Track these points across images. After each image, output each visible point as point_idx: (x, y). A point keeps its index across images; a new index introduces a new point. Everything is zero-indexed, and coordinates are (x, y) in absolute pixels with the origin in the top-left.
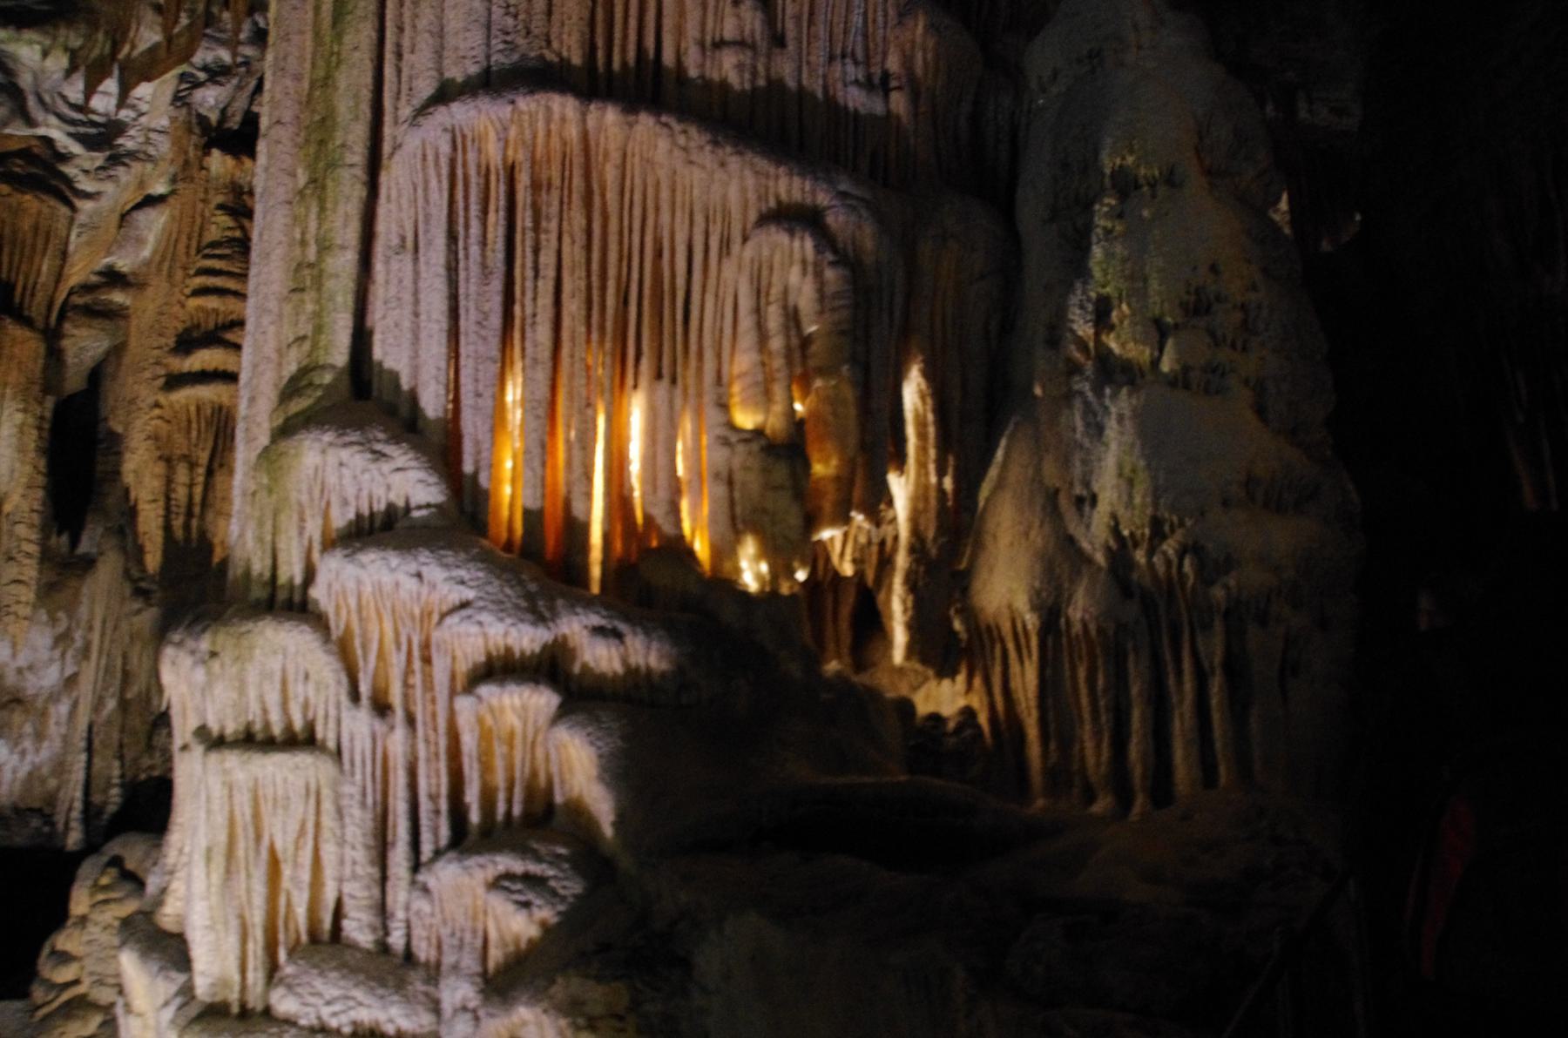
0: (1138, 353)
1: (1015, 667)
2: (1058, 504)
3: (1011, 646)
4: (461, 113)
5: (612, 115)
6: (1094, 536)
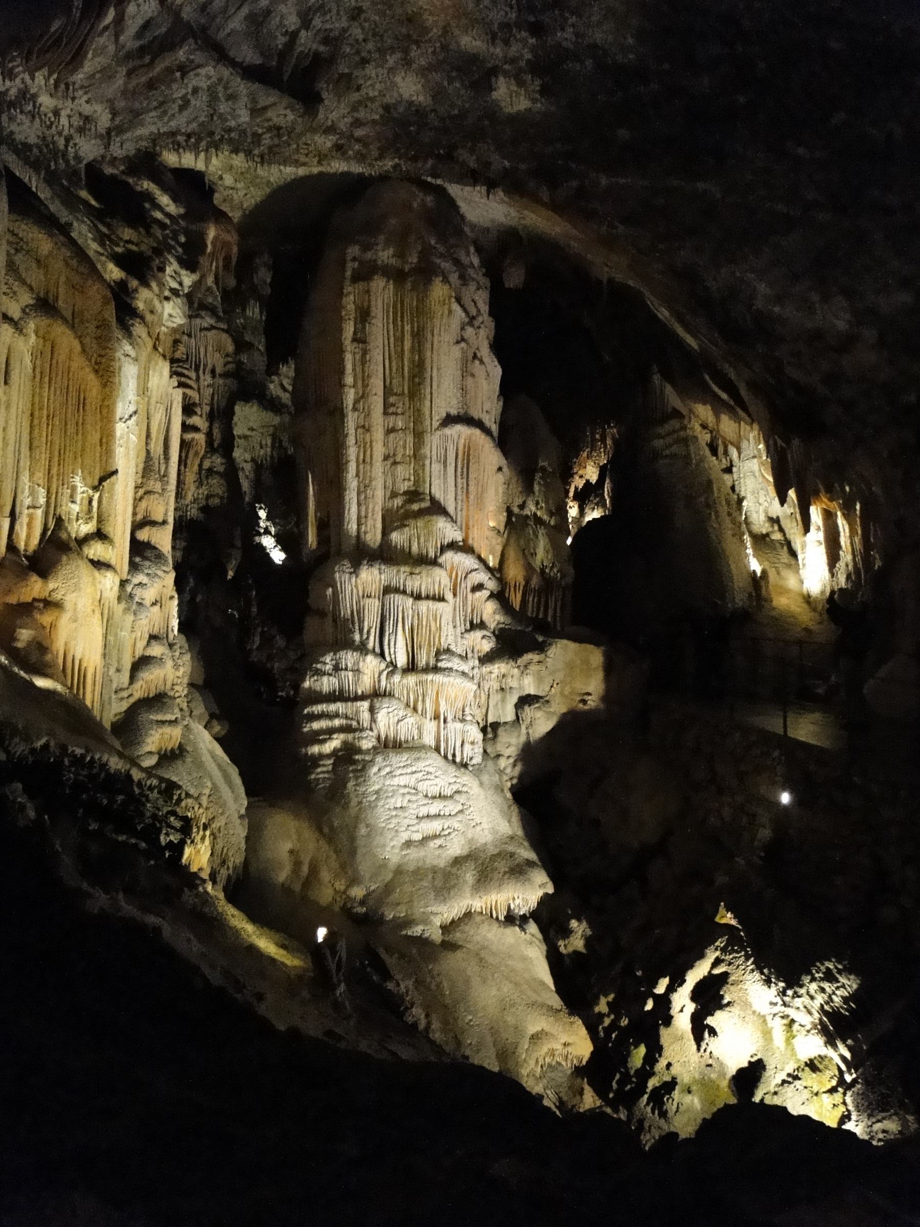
2: (527, 554)
3: (512, 589)
4: (459, 428)
6: (537, 563)
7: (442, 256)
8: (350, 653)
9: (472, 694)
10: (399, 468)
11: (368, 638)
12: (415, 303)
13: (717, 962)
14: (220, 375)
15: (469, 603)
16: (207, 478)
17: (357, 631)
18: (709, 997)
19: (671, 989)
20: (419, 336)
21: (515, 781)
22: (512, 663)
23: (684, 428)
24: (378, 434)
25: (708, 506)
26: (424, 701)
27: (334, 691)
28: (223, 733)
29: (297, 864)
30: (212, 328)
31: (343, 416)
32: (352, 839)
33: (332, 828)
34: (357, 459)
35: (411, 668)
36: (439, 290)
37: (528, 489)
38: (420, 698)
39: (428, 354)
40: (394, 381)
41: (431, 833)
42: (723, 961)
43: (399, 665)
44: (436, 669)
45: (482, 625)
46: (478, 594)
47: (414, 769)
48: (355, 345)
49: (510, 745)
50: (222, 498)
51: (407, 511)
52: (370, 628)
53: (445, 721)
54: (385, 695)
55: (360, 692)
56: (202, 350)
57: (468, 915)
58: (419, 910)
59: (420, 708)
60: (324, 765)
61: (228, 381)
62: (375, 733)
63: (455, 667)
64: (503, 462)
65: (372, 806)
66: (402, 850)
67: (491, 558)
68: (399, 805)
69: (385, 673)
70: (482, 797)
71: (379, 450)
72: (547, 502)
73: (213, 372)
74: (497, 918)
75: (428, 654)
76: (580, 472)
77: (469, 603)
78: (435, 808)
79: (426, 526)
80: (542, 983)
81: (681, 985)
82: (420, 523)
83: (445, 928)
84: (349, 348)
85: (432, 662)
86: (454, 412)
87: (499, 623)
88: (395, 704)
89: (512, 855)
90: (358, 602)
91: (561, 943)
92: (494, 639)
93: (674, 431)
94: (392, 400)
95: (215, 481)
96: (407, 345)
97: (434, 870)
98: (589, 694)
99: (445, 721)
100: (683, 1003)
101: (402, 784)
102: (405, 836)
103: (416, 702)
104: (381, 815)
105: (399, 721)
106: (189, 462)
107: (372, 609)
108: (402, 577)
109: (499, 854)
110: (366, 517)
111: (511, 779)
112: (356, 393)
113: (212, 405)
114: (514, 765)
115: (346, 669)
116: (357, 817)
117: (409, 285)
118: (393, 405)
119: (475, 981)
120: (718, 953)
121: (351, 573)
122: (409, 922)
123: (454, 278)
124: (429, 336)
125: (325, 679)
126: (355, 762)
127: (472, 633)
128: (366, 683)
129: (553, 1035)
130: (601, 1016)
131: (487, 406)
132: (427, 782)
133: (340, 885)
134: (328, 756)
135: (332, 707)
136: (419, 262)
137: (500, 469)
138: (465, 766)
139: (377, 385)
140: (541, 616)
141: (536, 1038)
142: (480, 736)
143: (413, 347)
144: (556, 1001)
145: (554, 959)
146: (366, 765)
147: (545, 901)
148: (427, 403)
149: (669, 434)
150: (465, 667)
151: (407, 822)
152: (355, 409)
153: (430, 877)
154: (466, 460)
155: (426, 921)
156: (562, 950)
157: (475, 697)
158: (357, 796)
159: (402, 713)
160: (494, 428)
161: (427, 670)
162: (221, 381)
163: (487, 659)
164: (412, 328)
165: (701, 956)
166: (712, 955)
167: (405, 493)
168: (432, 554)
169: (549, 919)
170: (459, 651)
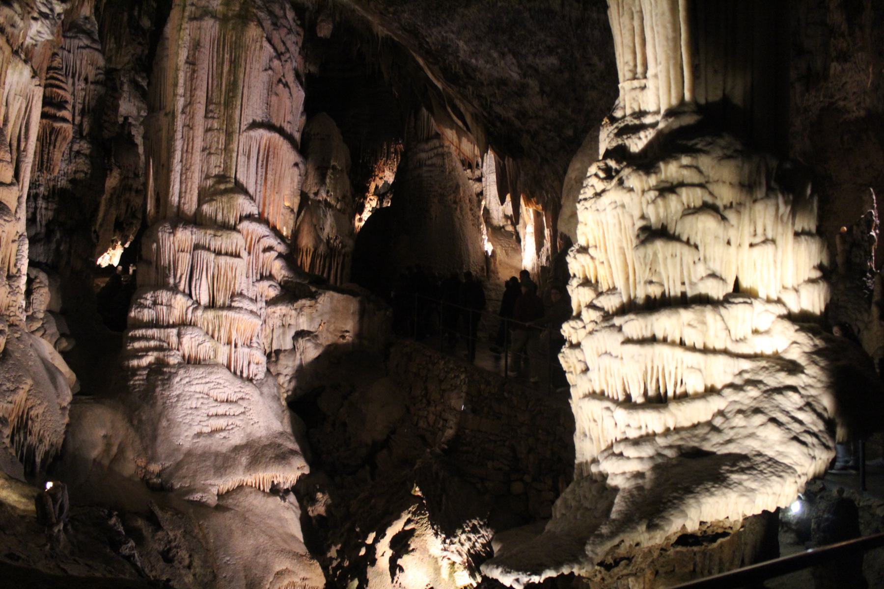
0: (333, 202)
1: (305, 257)
2: (317, 229)
5: (282, 139)
6: (324, 236)
7: (259, 8)
8: (164, 293)
9: (259, 327)
10: (213, 158)
11: (180, 282)
12: (234, 39)
13: (409, 521)
14: (92, 83)
15: (261, 260)
16: (75, 157)
17: (172, 276)
18: (401, 545)
19: (376, 540)
20: (235, 64)
21: (290, 393)
22: (290, 306)
23: (442, 146)
24: (199, 131)
25: (455, 202)
26: (219, 330)
27: (153, 320)
28: (70, 347)
29: (109, 446)
30: (87, 47)
31: (174, 117)
32: (155, 429)
33: (140, 421)
34: (182, 150)
35: (212, 305)
36: (253, 31)
37: (322, 181)
38: (217, 329)
39: (242, 76)
40: (214, 94)
41: (219, 427)
42: (413, 521)
43: (202, 303)
44: (230, 308)
45: (271, 277)
46: (267, 254)
47: (207, 380)
48: (187, 66)
49: (287, 367)
50: (86, 174)
51: (215, 190)
52: (182, 275)
53: (236, 346)
54: (190, 325)
55: (171, 322)
56: (78, 63)
57: (240, 487)
58: (201, 481)
59: (216, 336)
60: (140, 375)
61: (99, 87)
62: (181, 353)
63: (245, 307)
64: (298, 159)
65: (173, 406)
66: (193, 438)
67: (285, 229)
68: (194, 406)
69: (191, 308)
70: (261, 403)
71: (199, 143)
72: (335, 192)
73: (86, 80)
74: (264, 490)
75: (225, 296)
76: (380, 175)
77: (261, 260)
78: (222, 409)
79: (229, 201)
80: (294, 537)
81: (383, 537)
82: (225, 199)
83: (220, 496)
84: (182, 68)
85: (228, 302)
86: (259, 119)
87: (284, 277)
88: (196, 332)
89: (280, 445)
90: (174, 256)
91: (310, 509)
92: (279, 288)
93: (436, 148)
94: (211, 107)
95: (80, 161)
96: (226, 68)
97: (217, 454)
98: (347, 331)
99: (236, 346)
100: (384, 549)
101: (198, 390)
102: (196, 429)
103: (213, 331)
104: (180, 413)
105: (199, 344)
106: (58, 144)
107: (184, 260)
108: (208, 238)
109: (270, 445)
110: (185, 192)
111: (287, 391)
112: (186, 101)
113: (84, 103)
114: (290, 381)
115: (162, 304)
116: (160, 414)
117: (230, 26)
118: (211, 111)
119: (237, 534)
120: (410, 515)
121: (170, 233)
122: (191, 490)
123: (267, 24)
124: (243, 63)
125: (146, 311)
126: (163, 373)
127: (261, 282)
128: (175, 316)
129: (294, 572)
130: (331, 559)
131: (289, 118)
132: (216, 391)
133: (142, 462)
134: (144, 368)
135: (150, 332)
136: (241, 9)
137: (296, 165)
138: (250, 380)
139: (201, 96)
140: (325, 275)
141: (280, 574)
142: (264, 359)
143: (230, 71)
144: (302, 549)
145: (306, 522)
146: (171, 376)
147: (302, 479)
148: (238, 112)
149: (432, 149)
150: (253, 307)
151: (199, 418)
152: (183, 112)
153: (213, 458)
154: (267, 157)
155: (204, 490)
156: (310, 514)
157: (262, 330)
158: (163, 398)
159: (201, 339)
160: (297, 136)
161: (223, 308)
162: (92, 87)
163: (271, 302)
164: (231, 56)
165: (398, 517)
166: (405, 517)
167: (216, 176)
168: (232, 222)
169: (303, 492)
170: (250, 296)
